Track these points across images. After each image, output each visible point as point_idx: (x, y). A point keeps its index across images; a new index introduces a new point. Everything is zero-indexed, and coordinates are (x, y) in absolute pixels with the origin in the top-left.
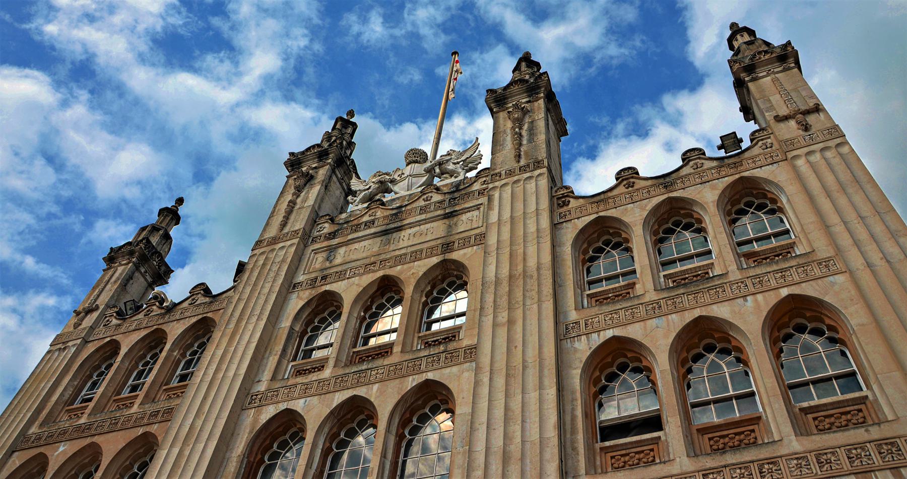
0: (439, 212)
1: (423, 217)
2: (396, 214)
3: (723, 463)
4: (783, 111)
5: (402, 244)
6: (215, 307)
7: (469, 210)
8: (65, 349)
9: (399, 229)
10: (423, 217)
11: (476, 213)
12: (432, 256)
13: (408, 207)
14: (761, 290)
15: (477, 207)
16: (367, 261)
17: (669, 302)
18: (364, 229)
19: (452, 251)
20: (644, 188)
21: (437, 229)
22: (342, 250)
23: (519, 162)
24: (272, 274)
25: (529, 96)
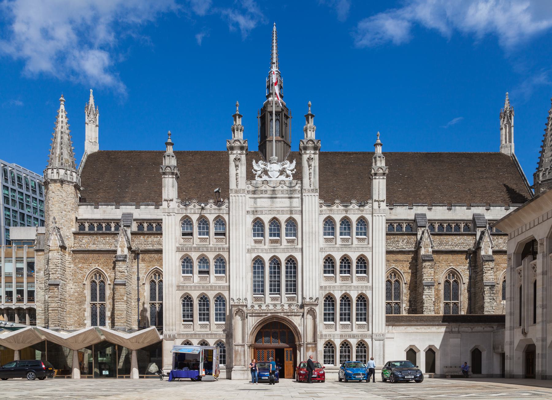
5: (278, 205)
6: (221, 212)
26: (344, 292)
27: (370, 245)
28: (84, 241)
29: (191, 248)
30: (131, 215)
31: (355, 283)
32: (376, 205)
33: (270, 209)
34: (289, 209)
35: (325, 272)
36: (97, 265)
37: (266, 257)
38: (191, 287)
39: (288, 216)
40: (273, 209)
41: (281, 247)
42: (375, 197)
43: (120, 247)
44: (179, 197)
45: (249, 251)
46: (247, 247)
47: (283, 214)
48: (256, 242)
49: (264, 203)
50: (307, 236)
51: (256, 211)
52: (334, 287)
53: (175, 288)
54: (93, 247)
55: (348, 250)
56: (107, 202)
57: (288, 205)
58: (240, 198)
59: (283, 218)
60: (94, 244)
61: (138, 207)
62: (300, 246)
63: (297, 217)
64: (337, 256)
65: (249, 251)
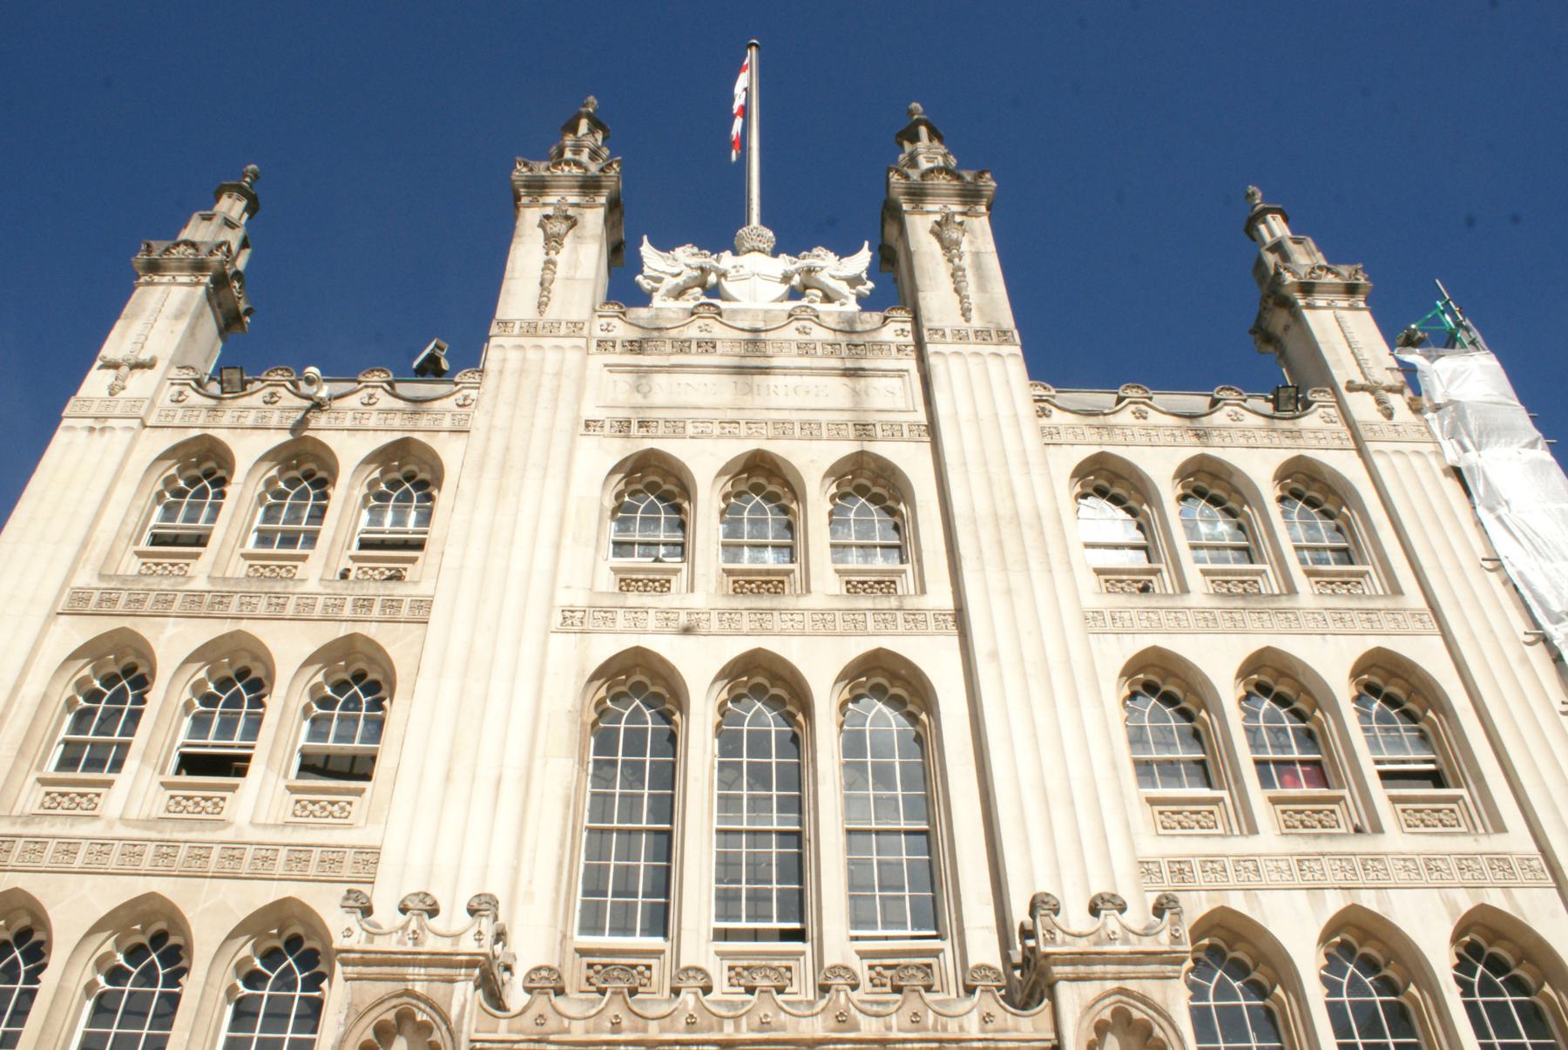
0: (834, 363)
1: (805, 362)
2: (754, 342)
3: (1318, 850)
4: (1360, 380)
6: (424, 422)
7: (885, 373)
8: (103, 429)
9: (764, 371)
10: (805, 362)
11: (896, 382)
12: (839, 437)
13: (770, 335)
14: (1344, 631)
15: (901, 373)
16: (721, 415)
17: (1226, 616)
18: (697, 353)
19: (871, 439)
20: (1166, 427)
21: (836, 391)
22: (660, 380)
23: (968, 320)
24: (545, 396)
25: (964, 203)
26: (1334, 903)
27: (1413, 596)
29: (165, 600)
31: (1395, 839)
33: (731, 415)
35: (1144, 769)
37: (699, 665)
39: (848, 448)
40: (749, 415)
41: (804, 602)
45: (572, 620)
46: (563, 599)
47: (811, 437)
48: (627, 582)
50: (987, 536)
51: (643, 424)
52: (1250, 863)
55: (1279, 622)
57: (846, 403)
58: (552, 357)
59: (813, 462)
64: (1218, 659)
65: (572, 620)
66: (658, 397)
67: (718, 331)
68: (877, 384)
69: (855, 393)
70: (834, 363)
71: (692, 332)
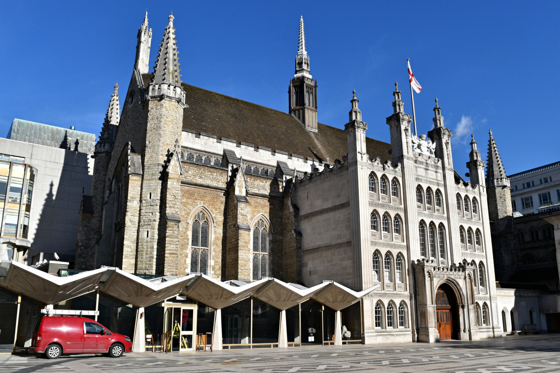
5: (430, 176)
9: (428, 170)
28: (190, 172)
30: (233, 153)
32: (481, 188)
33: (426, 179)
34: (435, 181)
36: (202, 202)
38: (380, 243)
42: (481, 184)
43: (239, 186)
44: (368, 152)
47: (434, 185)
49: (421, 172)
53: (369, 243)
54: (199, 181)
56: (210, 133)
60: (201, 177)
61: (239, 144)
62: (445, 215)
63: (442, 189)
66: (419, 174)
67: (423, 160)
68: (439, 175)
69: (437, 176)
70: (434, 170)
71: (420, 160)
